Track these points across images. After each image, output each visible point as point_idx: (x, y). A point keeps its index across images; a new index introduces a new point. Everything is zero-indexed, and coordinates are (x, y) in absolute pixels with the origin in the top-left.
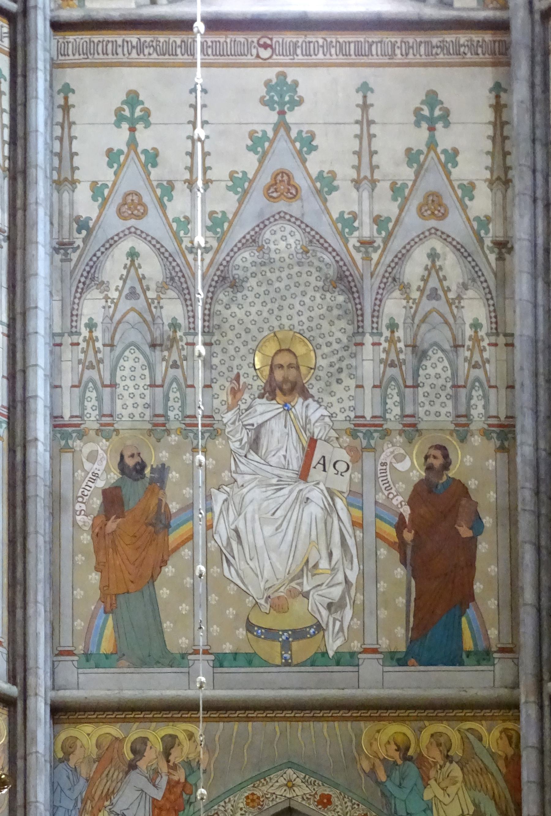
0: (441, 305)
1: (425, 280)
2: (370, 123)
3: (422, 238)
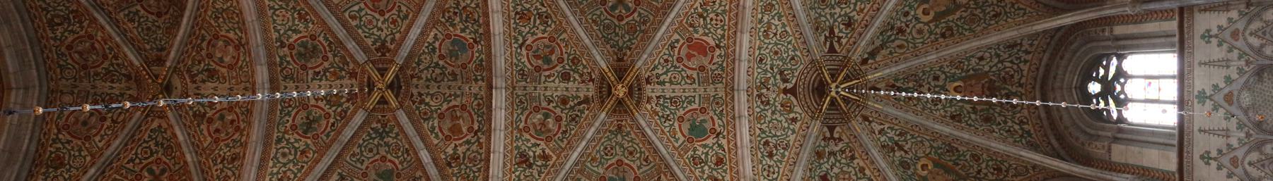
0: (1268, 30)
1: (1259, 37)
2: (1210, 62)
3: (1245, 39)
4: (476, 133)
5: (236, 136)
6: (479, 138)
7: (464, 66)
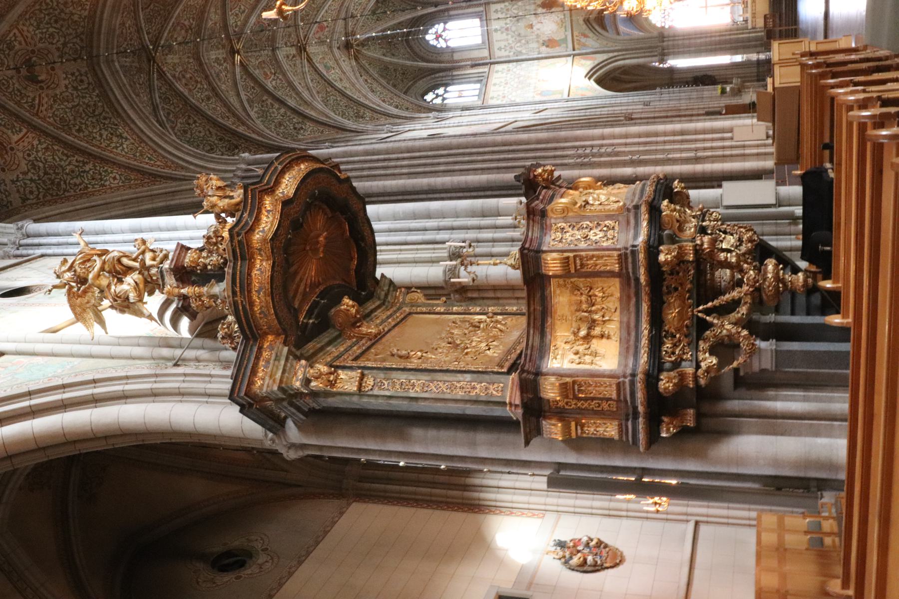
4: (275, 74)
5: (199, 86)
6: (278, 77)
7: (260, 40)
